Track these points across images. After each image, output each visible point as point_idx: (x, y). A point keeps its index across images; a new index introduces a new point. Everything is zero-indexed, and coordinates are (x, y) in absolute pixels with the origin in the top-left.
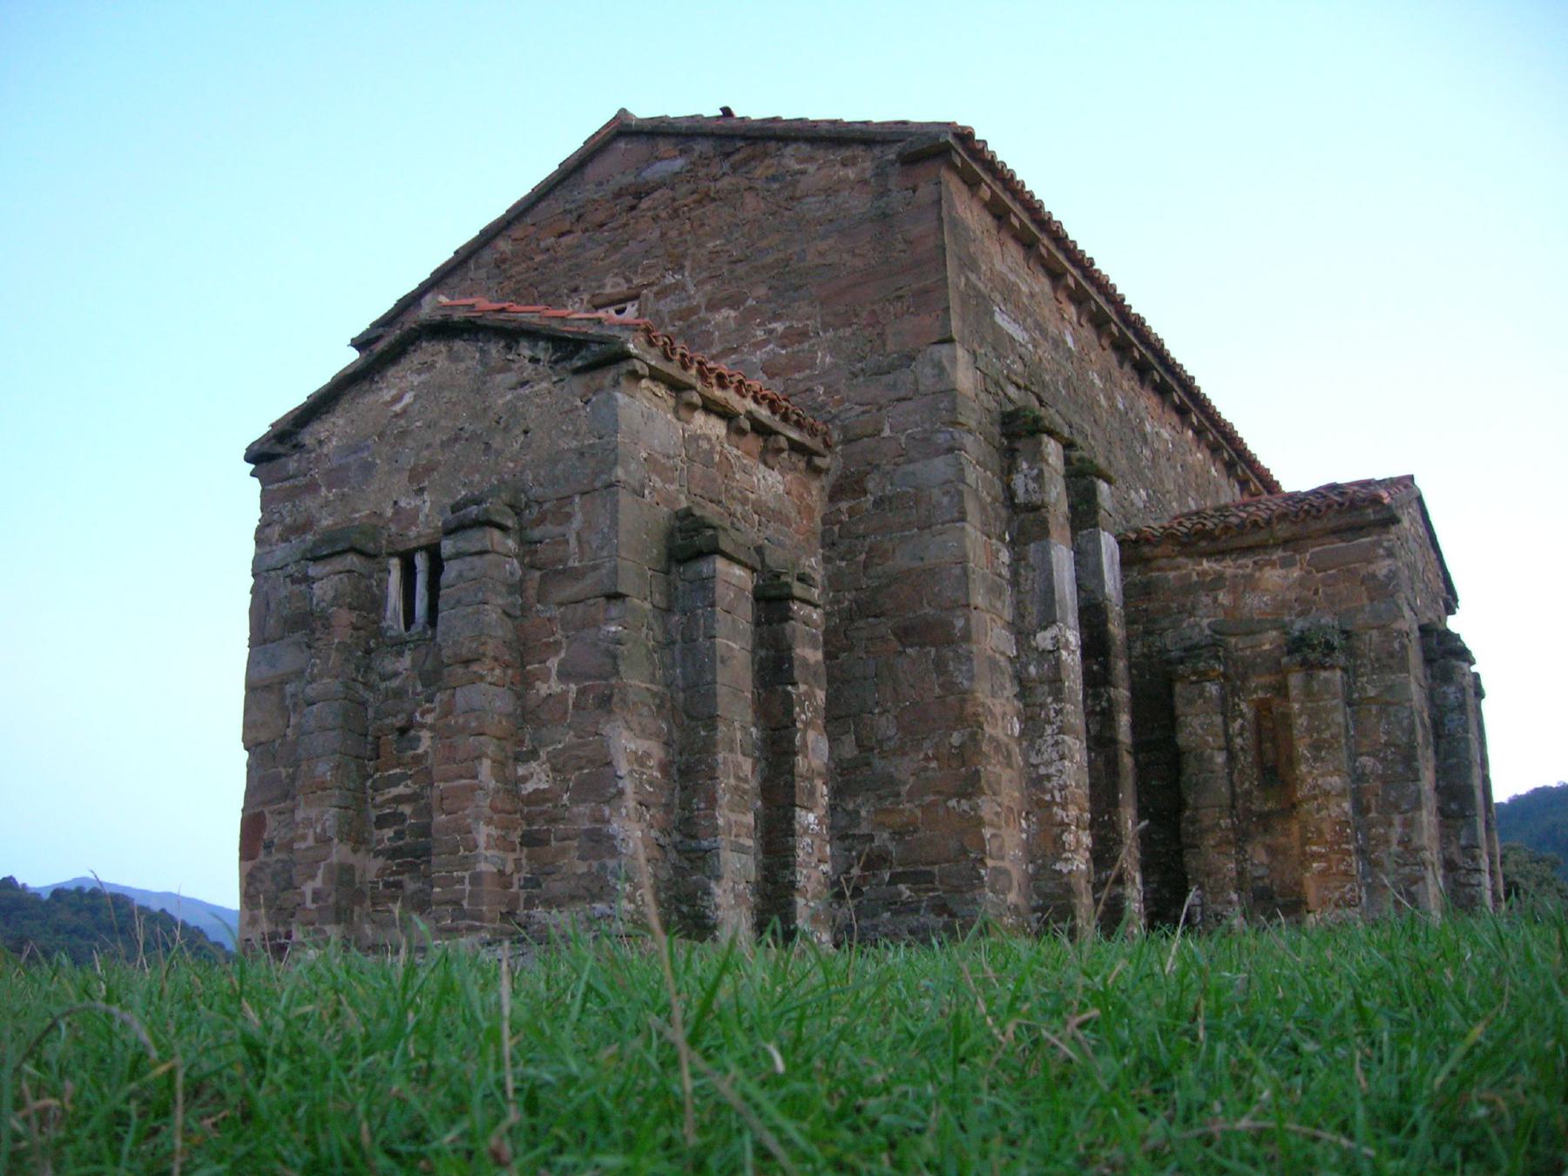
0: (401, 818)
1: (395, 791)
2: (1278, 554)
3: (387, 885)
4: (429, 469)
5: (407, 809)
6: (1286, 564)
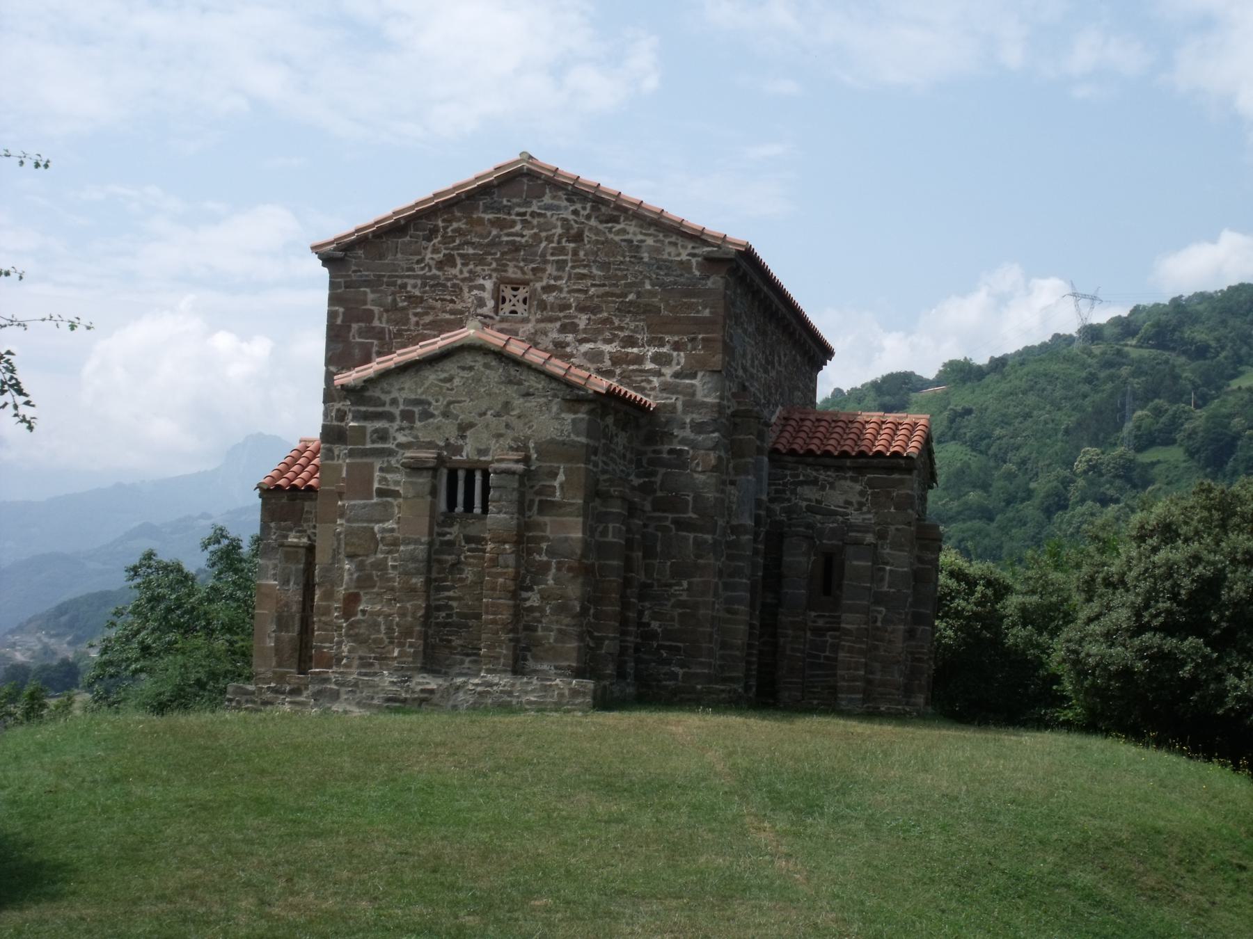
0: (451, 608)
1: (447, 594)
2: (850, 474)
3: (441, 640)
4: (471, 425)
5: (455, 604)
6: (854, 480)
